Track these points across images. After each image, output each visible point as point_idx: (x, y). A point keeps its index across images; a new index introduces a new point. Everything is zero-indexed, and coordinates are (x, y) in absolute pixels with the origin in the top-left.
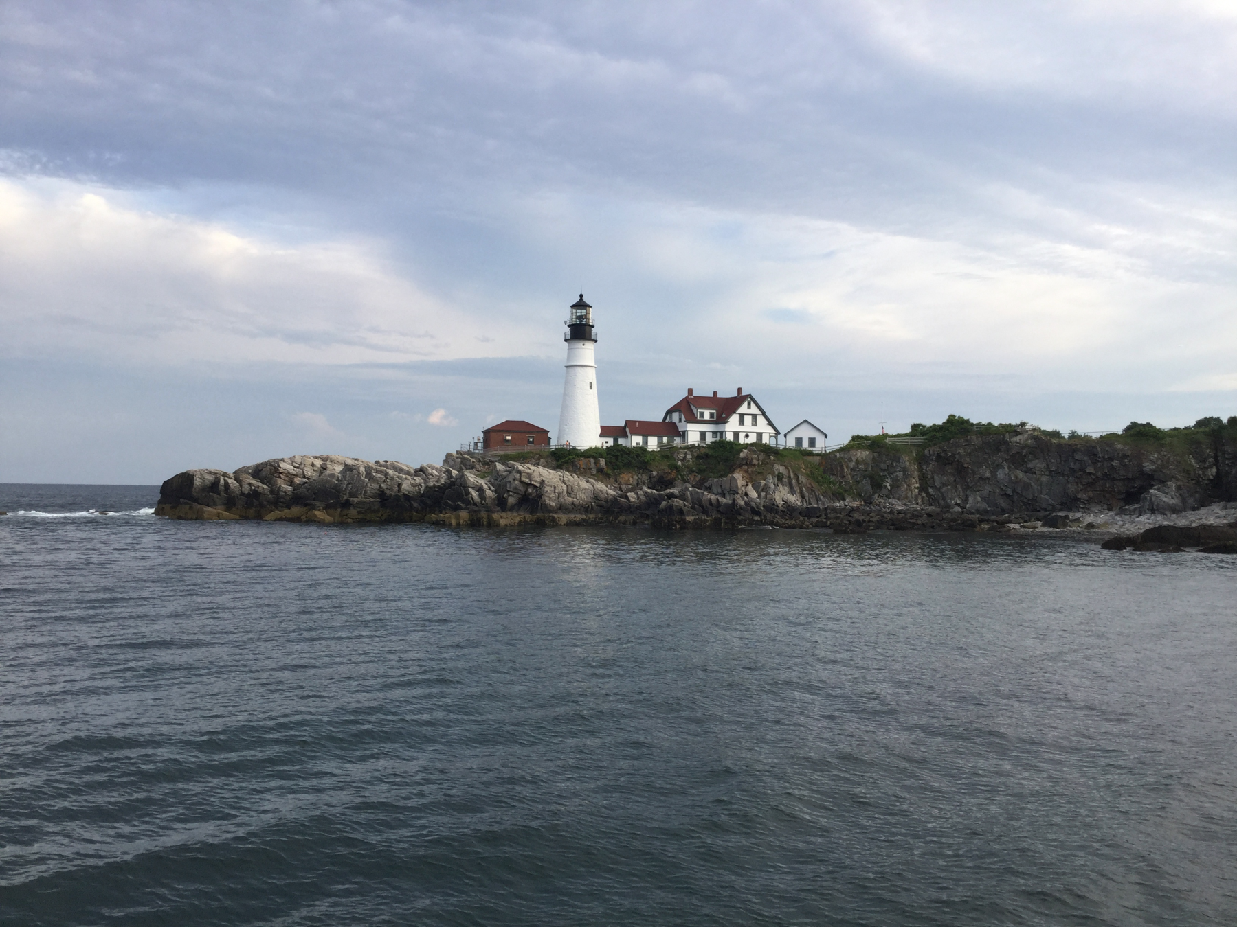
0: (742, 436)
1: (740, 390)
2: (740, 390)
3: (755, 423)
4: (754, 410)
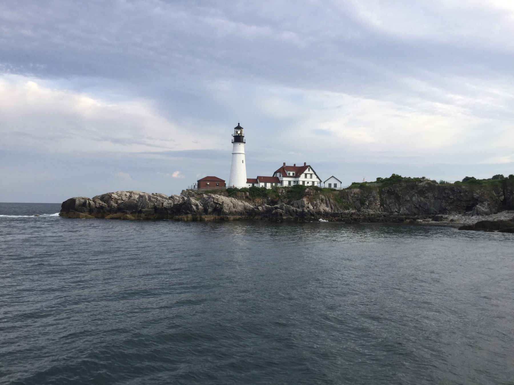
0: (306, 183)
1: (305, 163)
2: (305, 163)
3: (311, 177)
4: (311, 172)
